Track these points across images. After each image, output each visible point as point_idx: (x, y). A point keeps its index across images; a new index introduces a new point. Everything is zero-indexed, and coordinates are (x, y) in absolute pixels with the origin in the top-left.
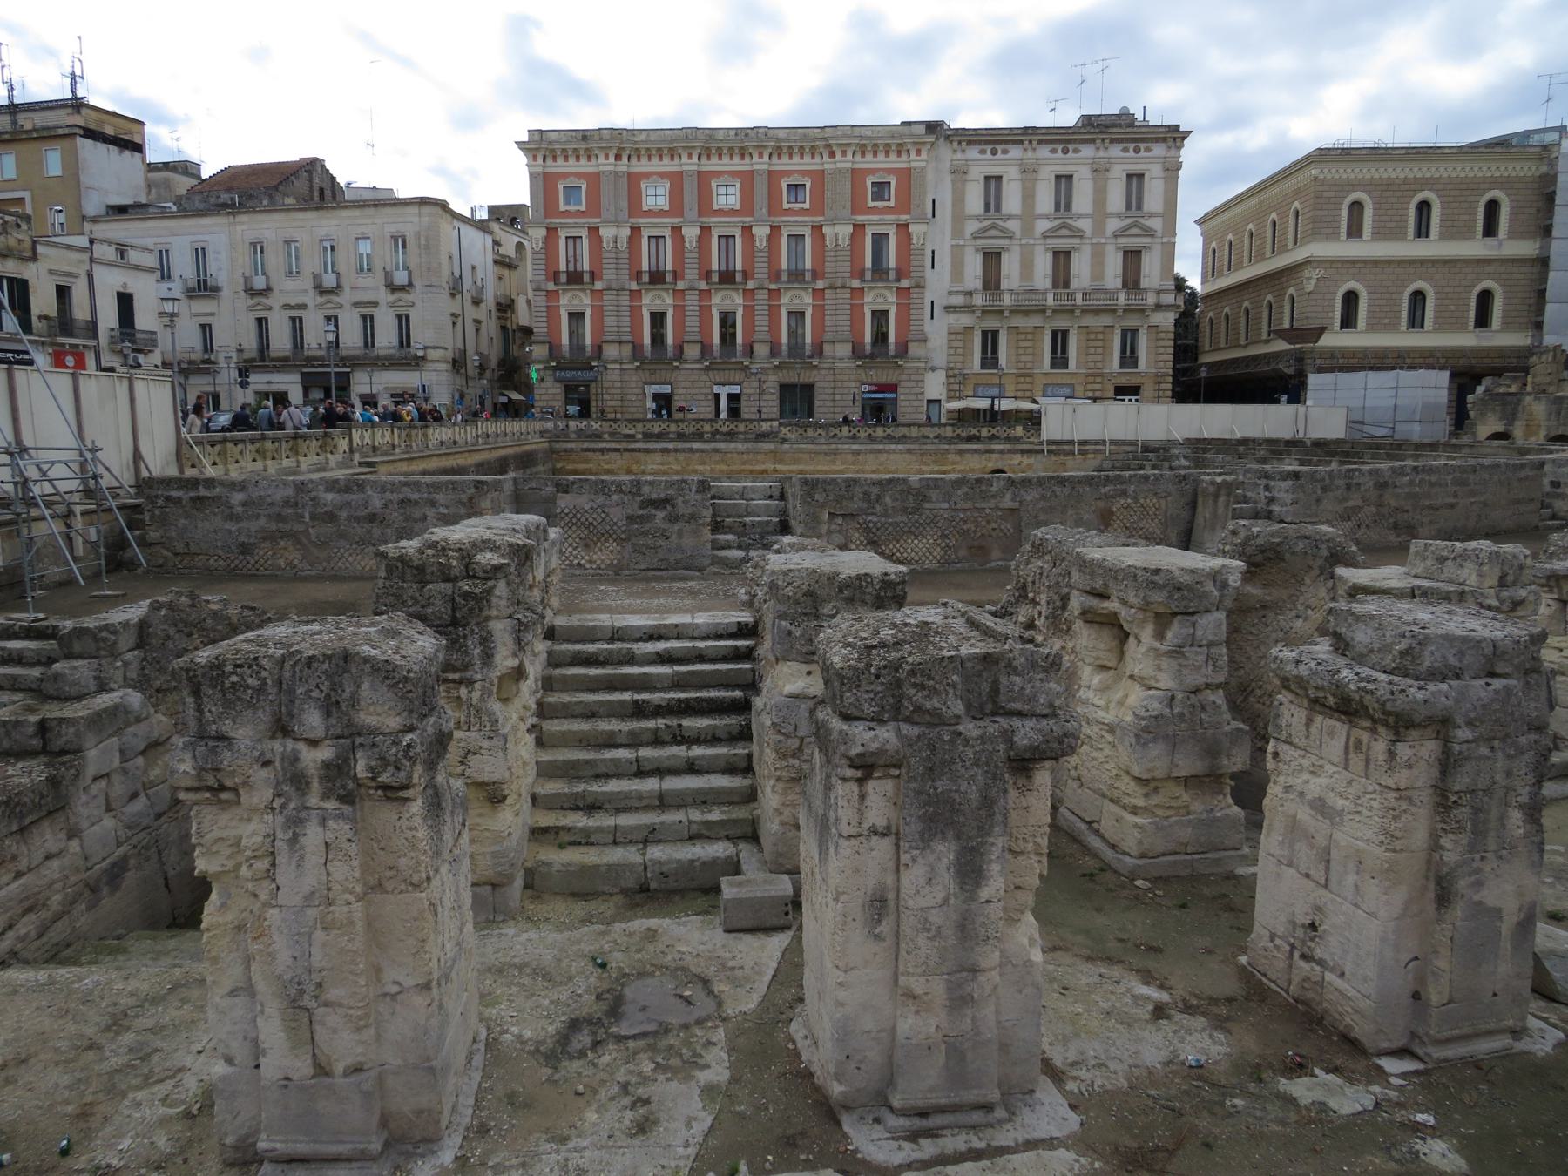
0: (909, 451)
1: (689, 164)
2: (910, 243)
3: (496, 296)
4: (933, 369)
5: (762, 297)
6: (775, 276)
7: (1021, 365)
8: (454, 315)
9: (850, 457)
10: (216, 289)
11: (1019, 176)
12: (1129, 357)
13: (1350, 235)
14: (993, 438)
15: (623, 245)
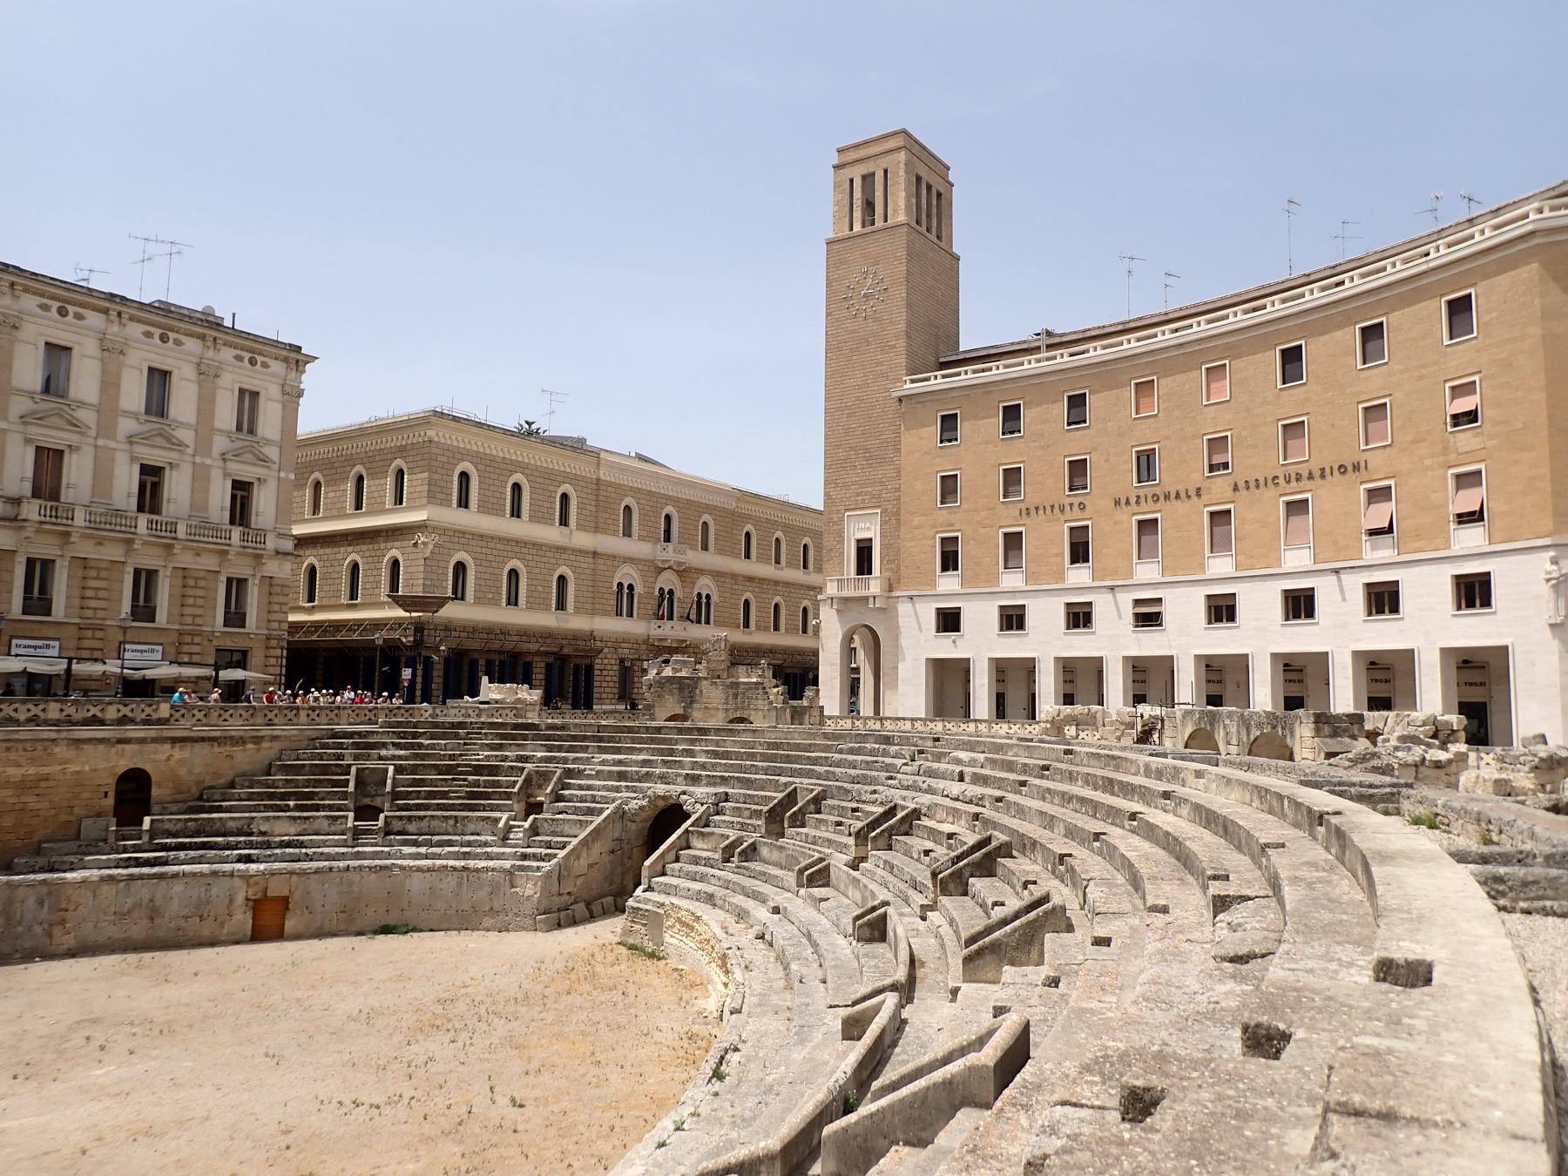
7: (89, 613)
11: (98, 353)
12: (235, 617)
13: (460, 505)
14: (124, 721)
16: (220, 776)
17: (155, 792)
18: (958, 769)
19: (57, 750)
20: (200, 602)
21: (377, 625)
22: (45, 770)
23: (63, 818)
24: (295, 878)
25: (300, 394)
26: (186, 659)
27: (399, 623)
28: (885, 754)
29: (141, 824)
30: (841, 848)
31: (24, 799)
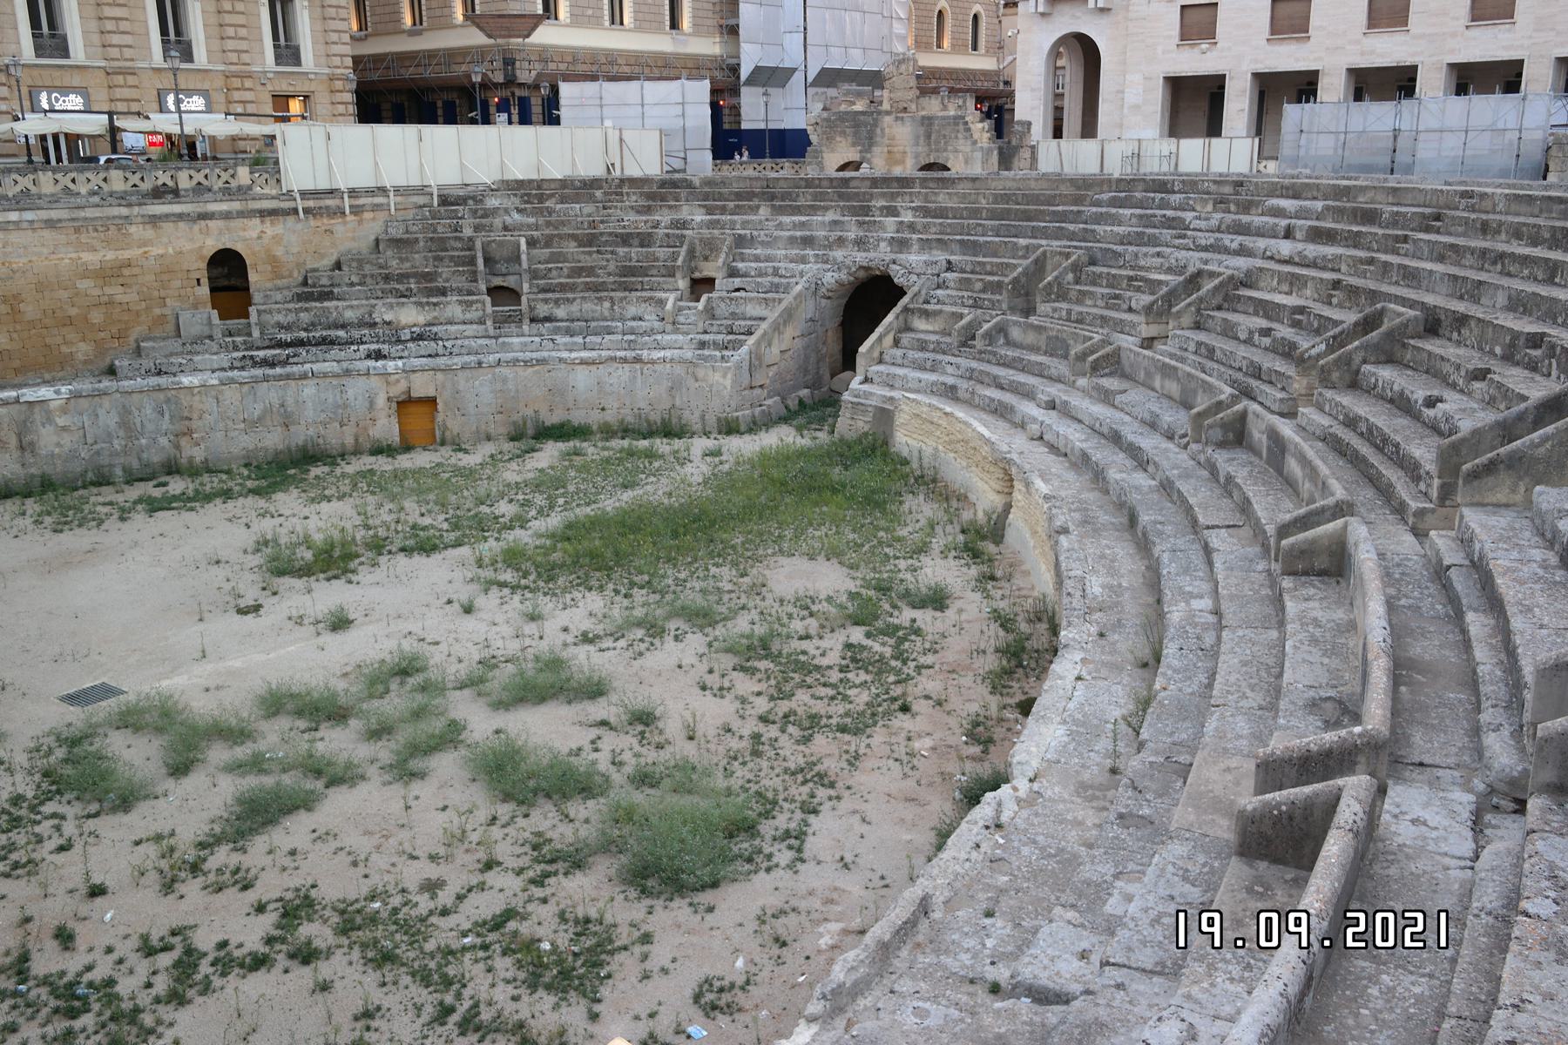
0: (50, 224)
7: (114, 52)
12: (288, 52)
16: (322, 256)
17: (253, 277)
18: (1284, 223)
19: (133, 229)
20: (243, 32)
21: (452, 55)
22: (126, 254)
23: (157, 311)
24: (440, 376)
26: (240, 110)
27: (480, 54)
28: (1164, 205)
29: (247, 316)
30: (1121, 327)
31: (108, 290)
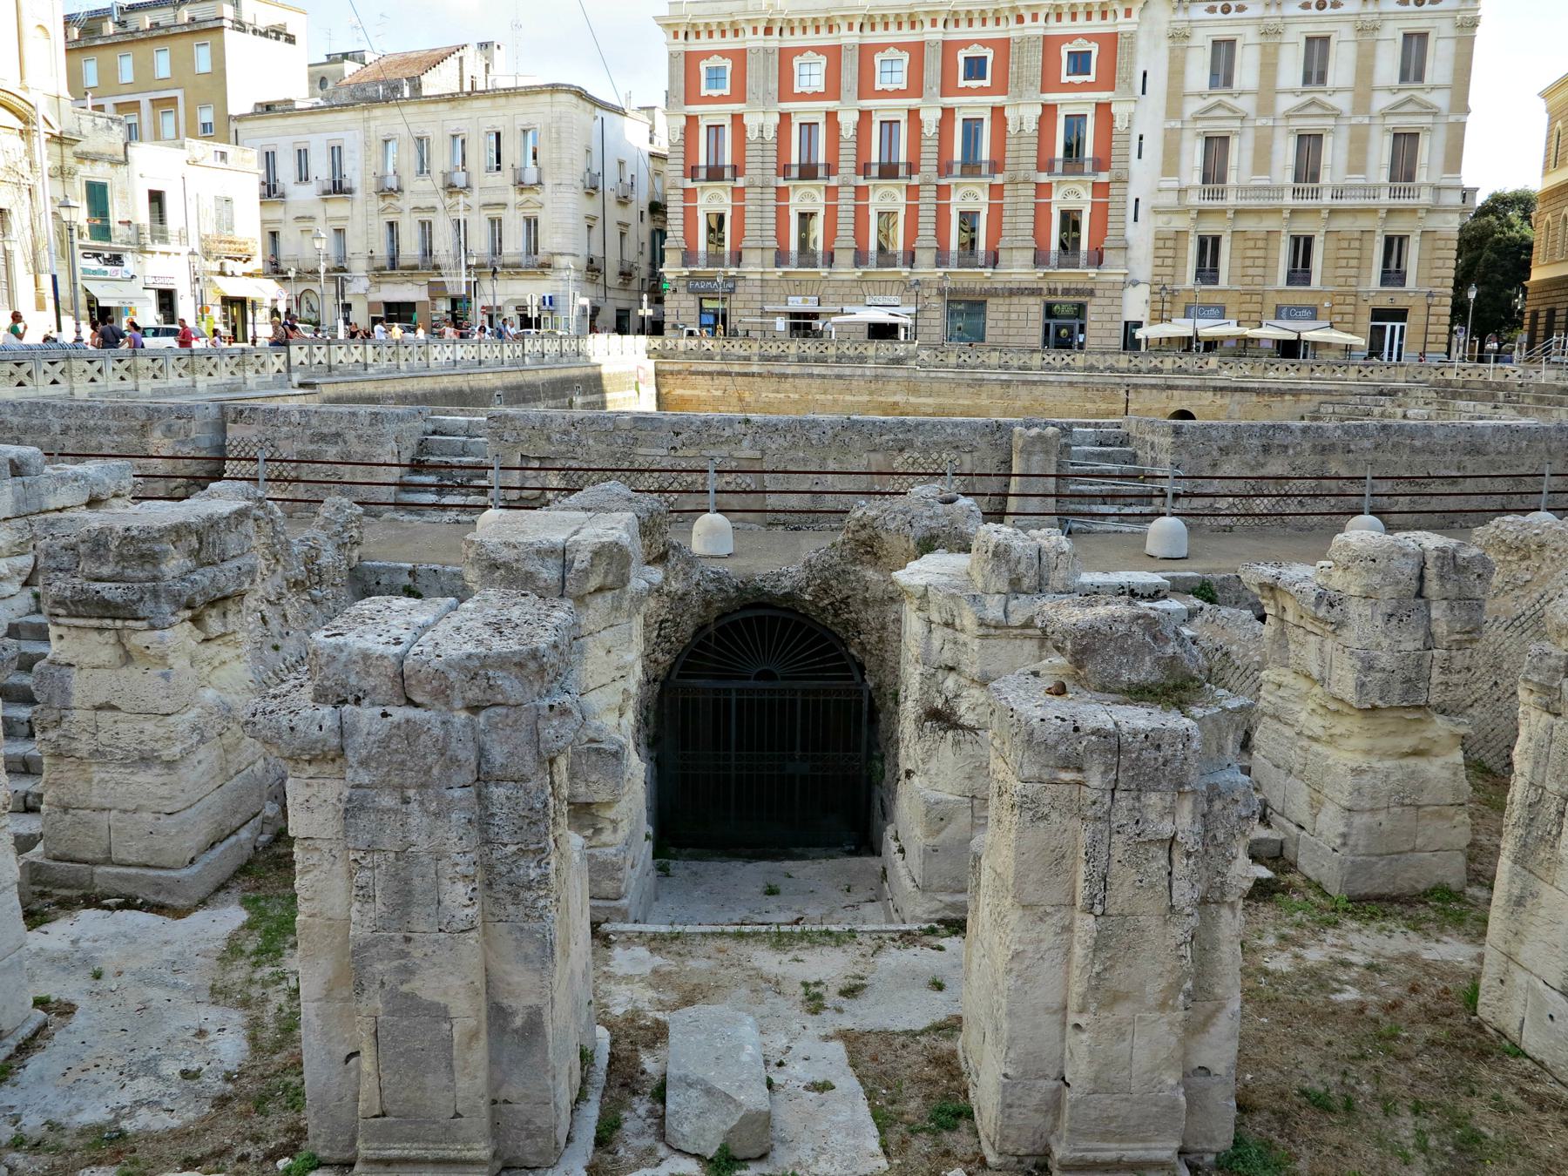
1: (848, 38)
2: (1111, 127)
3: (652, 192)
4: (1135, 283)
5: (928, 195)
6: (944, 168)
8: (595, 219)
9: (998, 390)
10: (350, 191)
11: (1258, 40)
12: (1393, 274)
15: (770, 134)
25: (1474, 24)
